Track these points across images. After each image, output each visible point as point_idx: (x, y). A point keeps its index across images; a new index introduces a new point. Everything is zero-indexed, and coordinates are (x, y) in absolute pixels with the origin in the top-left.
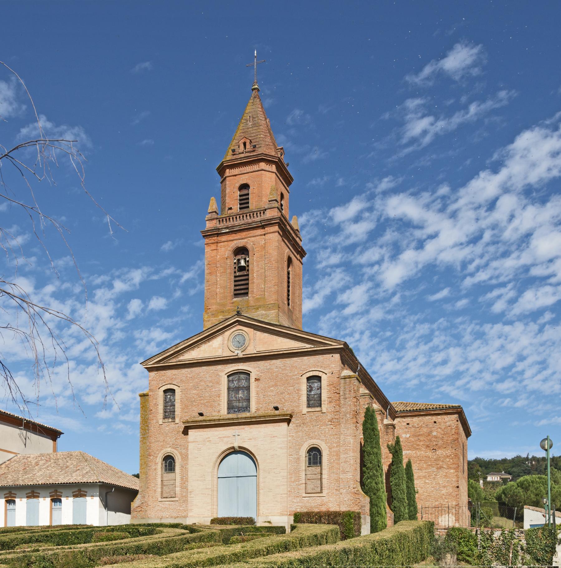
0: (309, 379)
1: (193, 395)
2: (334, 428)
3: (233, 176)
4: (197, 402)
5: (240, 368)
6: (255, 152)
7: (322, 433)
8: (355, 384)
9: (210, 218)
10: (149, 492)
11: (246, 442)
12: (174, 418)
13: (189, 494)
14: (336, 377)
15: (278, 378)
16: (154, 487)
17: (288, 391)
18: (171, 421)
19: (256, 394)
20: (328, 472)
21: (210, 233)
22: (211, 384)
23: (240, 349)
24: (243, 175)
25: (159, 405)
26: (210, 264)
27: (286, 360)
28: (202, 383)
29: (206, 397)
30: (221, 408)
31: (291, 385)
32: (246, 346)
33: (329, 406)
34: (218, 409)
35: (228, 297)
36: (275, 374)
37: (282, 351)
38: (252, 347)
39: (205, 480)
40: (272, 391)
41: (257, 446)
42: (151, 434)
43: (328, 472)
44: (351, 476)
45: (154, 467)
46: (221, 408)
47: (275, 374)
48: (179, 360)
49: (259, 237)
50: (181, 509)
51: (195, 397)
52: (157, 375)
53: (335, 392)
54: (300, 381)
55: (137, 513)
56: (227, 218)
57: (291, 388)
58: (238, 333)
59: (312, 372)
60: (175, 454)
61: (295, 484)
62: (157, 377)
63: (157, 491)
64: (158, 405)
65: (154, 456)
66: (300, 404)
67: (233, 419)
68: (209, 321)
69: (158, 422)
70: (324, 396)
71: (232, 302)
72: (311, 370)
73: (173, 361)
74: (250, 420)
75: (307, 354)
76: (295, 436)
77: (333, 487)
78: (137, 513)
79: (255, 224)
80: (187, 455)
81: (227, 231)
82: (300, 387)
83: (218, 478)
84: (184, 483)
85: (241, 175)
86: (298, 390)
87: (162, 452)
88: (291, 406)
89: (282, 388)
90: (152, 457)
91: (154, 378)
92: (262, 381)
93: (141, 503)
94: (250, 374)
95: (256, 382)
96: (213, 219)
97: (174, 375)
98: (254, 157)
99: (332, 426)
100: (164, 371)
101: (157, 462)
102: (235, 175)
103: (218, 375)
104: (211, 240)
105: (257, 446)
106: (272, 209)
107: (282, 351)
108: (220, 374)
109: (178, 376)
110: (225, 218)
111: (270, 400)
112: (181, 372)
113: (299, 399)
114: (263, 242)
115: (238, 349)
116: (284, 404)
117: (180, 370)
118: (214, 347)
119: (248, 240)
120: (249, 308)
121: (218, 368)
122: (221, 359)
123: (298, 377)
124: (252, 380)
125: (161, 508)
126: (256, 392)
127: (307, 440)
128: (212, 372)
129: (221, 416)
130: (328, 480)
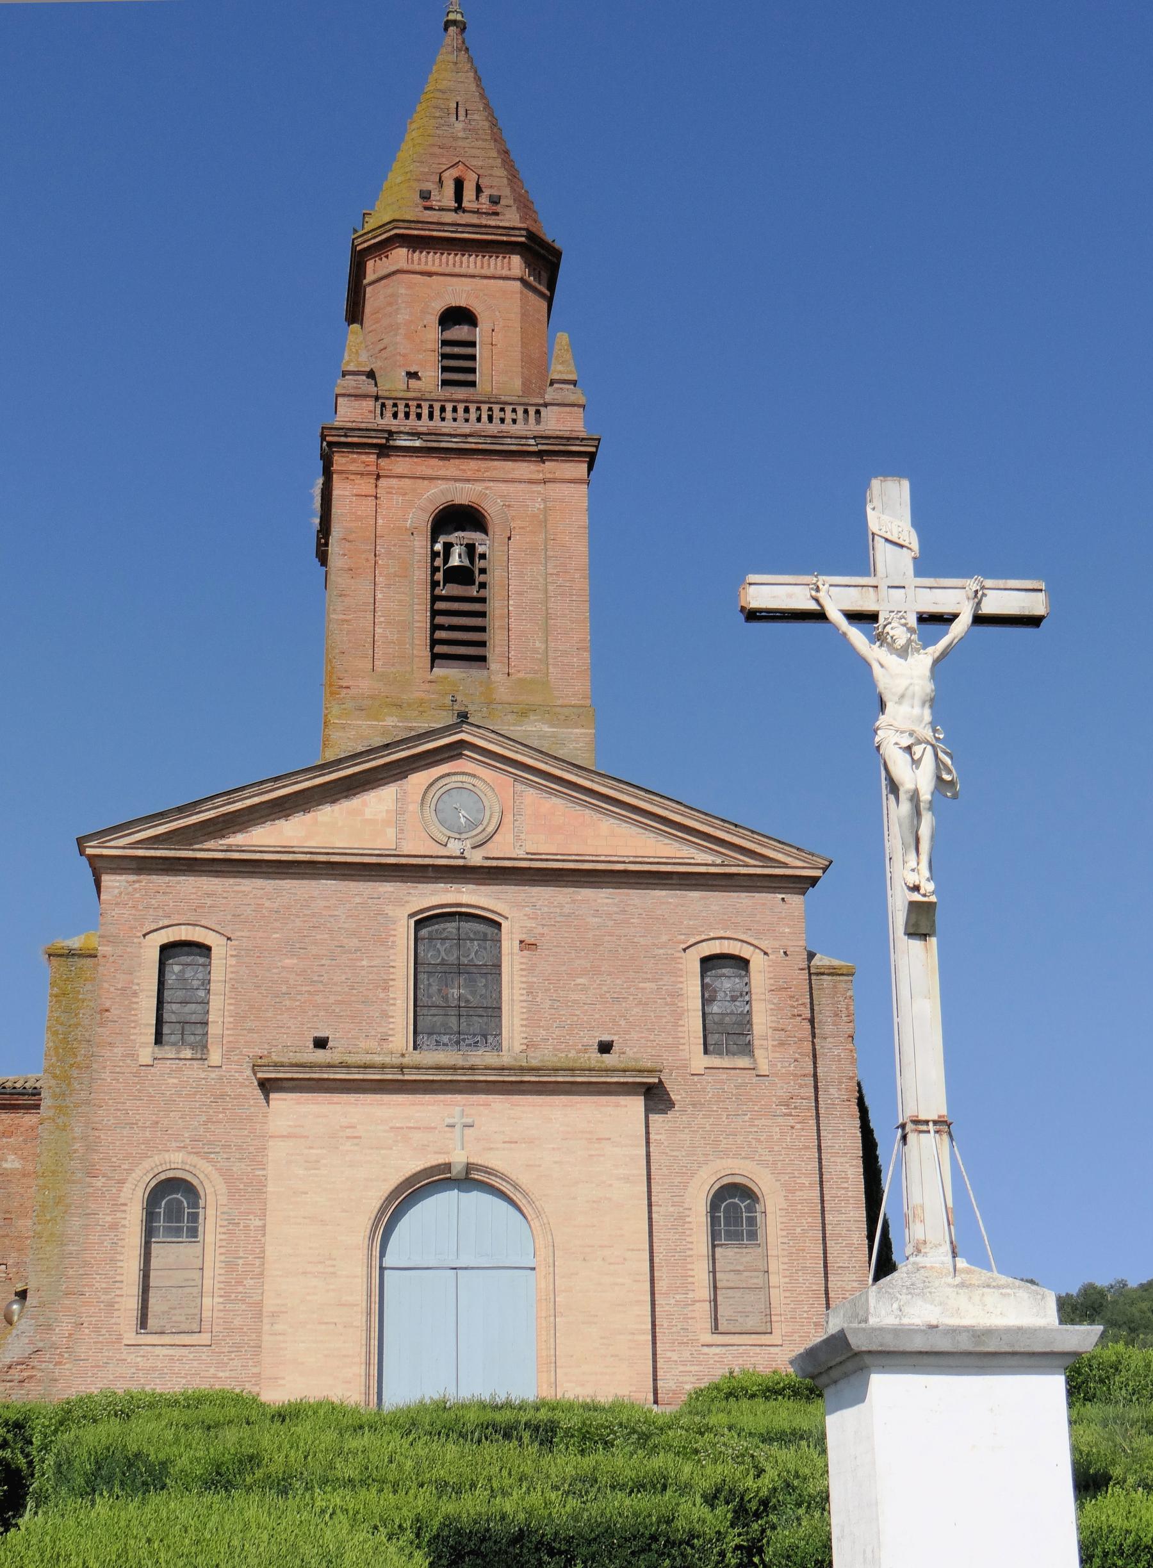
0: (708, 962)
1: (284, 974)
2: (798, 1126)
3: (422, 273)
4: (299, 997)
5: (465, 899)
6: (500, 217)
7: (759, 1141)
8: (849, 993)
9: (352, 391)
10: (83, 1309)
11: (497, 1149)
12: (202, 1047)
13: (265, 1320)
14: (796, 967)
15: (601, 948)
16: (106, 1291)
17: (640, 996)
18: (189, 1056)
19: (524, 992)
20: (785, 1267)
21: (355, 440)
22: (355, 941)
23: (464, 836)
24: (455, 279)
25: (142, 995)
26: (350, 538)
27: (628, 895)
28: (318, 937)
29: (335, 984)
30: (391, 1026)
31: (649, 976)
32: (491, 829)
33: (777, 1055)
34: (380, 1030)
35: (417, 659)
36: (590, 935)
37: (624, 862)
38: (510, 838)
39: (334, 1273)
40: (584, 989)
41: (540, 1166)
42: (102, 1096)
43: (785, 1267)
44: (855, 1284)
45: (109, 1219)
46: (391, 1026)
47: (590, 935)
48: (231, 845)
49: (523, 486)
50: (221, 1374)
51: (292, 982)
52: (137, 885)
53: (796, 1012)
54: (680, 966)
55: (11, 1388)
56: (411, 403)
57: (647, 985)
58: (460, 785)
59: (717, 942)
60: (201, 1176)
61: (672, 1301)
62: (137, 895)
63: (116, 1306)
64: (135, 994)
65: (109, 1178)
66: (682, 1041)
67: (454, 1068)
68: (343, 727)
69: (134, 1056)
70: (762, 1021)
71: (430, 677)
72: (712, 935)
73: (212, 849)
74: (449, 1078)
75: (702, 881)
76: (666, 1144)
77: (805, 1315)
78: (11, 1388)
79: (514, 441)
80: (259, 1187)
81: (417, 443)
82: (680, 986)
83: (534, 1269)
84: (240, 1283)
85: (449, 278)
86: (672, 995)
87: (147, 1164)
88: (649, 1044)
89: (618, 981)
90: (103, 1180)
91: (125, 897)
92: (547, 952)
93: (32, 1348)
94: (499, 925)
95: (525, 952)
96: (365, 396)
97: (209, 895)
98: (500, 231)
99: (791, 1121)
100: (167, 879)
101: (122, 1201)
102: (430, 274)
103: (380, 913)
104: (354, 461)
105: (540, 1166)
106: (568, 409)
107: (624, 862)
108: (391, 914)
109: (224, 901)
110: (404, 402)
111: (575, 1018)
112: (236, 888)
113: (676, 1025)
114: (537, 505)
115: (458, 836)
116: (627, 1037)
117: (232, 881)
118: (368, 816)
119: (487, 488)
120: (494, 706)
121: (381, 889)
122: (403, 861)
123: (669, 952)
124: (509, 945)
125: (133, 1370)
126: (524, 986)
127: (711, 1158)
128: (358, 900)
129: (403, 1055)
130: (788, 1294)
